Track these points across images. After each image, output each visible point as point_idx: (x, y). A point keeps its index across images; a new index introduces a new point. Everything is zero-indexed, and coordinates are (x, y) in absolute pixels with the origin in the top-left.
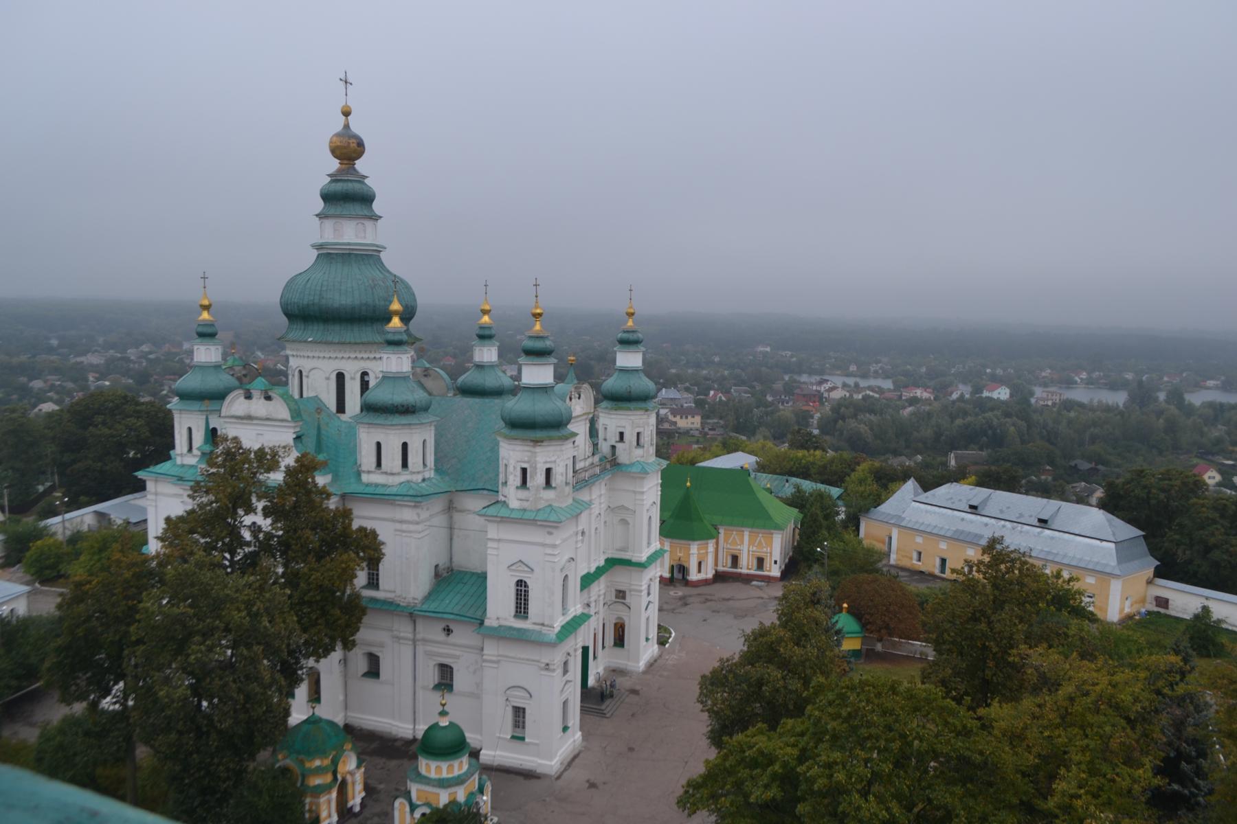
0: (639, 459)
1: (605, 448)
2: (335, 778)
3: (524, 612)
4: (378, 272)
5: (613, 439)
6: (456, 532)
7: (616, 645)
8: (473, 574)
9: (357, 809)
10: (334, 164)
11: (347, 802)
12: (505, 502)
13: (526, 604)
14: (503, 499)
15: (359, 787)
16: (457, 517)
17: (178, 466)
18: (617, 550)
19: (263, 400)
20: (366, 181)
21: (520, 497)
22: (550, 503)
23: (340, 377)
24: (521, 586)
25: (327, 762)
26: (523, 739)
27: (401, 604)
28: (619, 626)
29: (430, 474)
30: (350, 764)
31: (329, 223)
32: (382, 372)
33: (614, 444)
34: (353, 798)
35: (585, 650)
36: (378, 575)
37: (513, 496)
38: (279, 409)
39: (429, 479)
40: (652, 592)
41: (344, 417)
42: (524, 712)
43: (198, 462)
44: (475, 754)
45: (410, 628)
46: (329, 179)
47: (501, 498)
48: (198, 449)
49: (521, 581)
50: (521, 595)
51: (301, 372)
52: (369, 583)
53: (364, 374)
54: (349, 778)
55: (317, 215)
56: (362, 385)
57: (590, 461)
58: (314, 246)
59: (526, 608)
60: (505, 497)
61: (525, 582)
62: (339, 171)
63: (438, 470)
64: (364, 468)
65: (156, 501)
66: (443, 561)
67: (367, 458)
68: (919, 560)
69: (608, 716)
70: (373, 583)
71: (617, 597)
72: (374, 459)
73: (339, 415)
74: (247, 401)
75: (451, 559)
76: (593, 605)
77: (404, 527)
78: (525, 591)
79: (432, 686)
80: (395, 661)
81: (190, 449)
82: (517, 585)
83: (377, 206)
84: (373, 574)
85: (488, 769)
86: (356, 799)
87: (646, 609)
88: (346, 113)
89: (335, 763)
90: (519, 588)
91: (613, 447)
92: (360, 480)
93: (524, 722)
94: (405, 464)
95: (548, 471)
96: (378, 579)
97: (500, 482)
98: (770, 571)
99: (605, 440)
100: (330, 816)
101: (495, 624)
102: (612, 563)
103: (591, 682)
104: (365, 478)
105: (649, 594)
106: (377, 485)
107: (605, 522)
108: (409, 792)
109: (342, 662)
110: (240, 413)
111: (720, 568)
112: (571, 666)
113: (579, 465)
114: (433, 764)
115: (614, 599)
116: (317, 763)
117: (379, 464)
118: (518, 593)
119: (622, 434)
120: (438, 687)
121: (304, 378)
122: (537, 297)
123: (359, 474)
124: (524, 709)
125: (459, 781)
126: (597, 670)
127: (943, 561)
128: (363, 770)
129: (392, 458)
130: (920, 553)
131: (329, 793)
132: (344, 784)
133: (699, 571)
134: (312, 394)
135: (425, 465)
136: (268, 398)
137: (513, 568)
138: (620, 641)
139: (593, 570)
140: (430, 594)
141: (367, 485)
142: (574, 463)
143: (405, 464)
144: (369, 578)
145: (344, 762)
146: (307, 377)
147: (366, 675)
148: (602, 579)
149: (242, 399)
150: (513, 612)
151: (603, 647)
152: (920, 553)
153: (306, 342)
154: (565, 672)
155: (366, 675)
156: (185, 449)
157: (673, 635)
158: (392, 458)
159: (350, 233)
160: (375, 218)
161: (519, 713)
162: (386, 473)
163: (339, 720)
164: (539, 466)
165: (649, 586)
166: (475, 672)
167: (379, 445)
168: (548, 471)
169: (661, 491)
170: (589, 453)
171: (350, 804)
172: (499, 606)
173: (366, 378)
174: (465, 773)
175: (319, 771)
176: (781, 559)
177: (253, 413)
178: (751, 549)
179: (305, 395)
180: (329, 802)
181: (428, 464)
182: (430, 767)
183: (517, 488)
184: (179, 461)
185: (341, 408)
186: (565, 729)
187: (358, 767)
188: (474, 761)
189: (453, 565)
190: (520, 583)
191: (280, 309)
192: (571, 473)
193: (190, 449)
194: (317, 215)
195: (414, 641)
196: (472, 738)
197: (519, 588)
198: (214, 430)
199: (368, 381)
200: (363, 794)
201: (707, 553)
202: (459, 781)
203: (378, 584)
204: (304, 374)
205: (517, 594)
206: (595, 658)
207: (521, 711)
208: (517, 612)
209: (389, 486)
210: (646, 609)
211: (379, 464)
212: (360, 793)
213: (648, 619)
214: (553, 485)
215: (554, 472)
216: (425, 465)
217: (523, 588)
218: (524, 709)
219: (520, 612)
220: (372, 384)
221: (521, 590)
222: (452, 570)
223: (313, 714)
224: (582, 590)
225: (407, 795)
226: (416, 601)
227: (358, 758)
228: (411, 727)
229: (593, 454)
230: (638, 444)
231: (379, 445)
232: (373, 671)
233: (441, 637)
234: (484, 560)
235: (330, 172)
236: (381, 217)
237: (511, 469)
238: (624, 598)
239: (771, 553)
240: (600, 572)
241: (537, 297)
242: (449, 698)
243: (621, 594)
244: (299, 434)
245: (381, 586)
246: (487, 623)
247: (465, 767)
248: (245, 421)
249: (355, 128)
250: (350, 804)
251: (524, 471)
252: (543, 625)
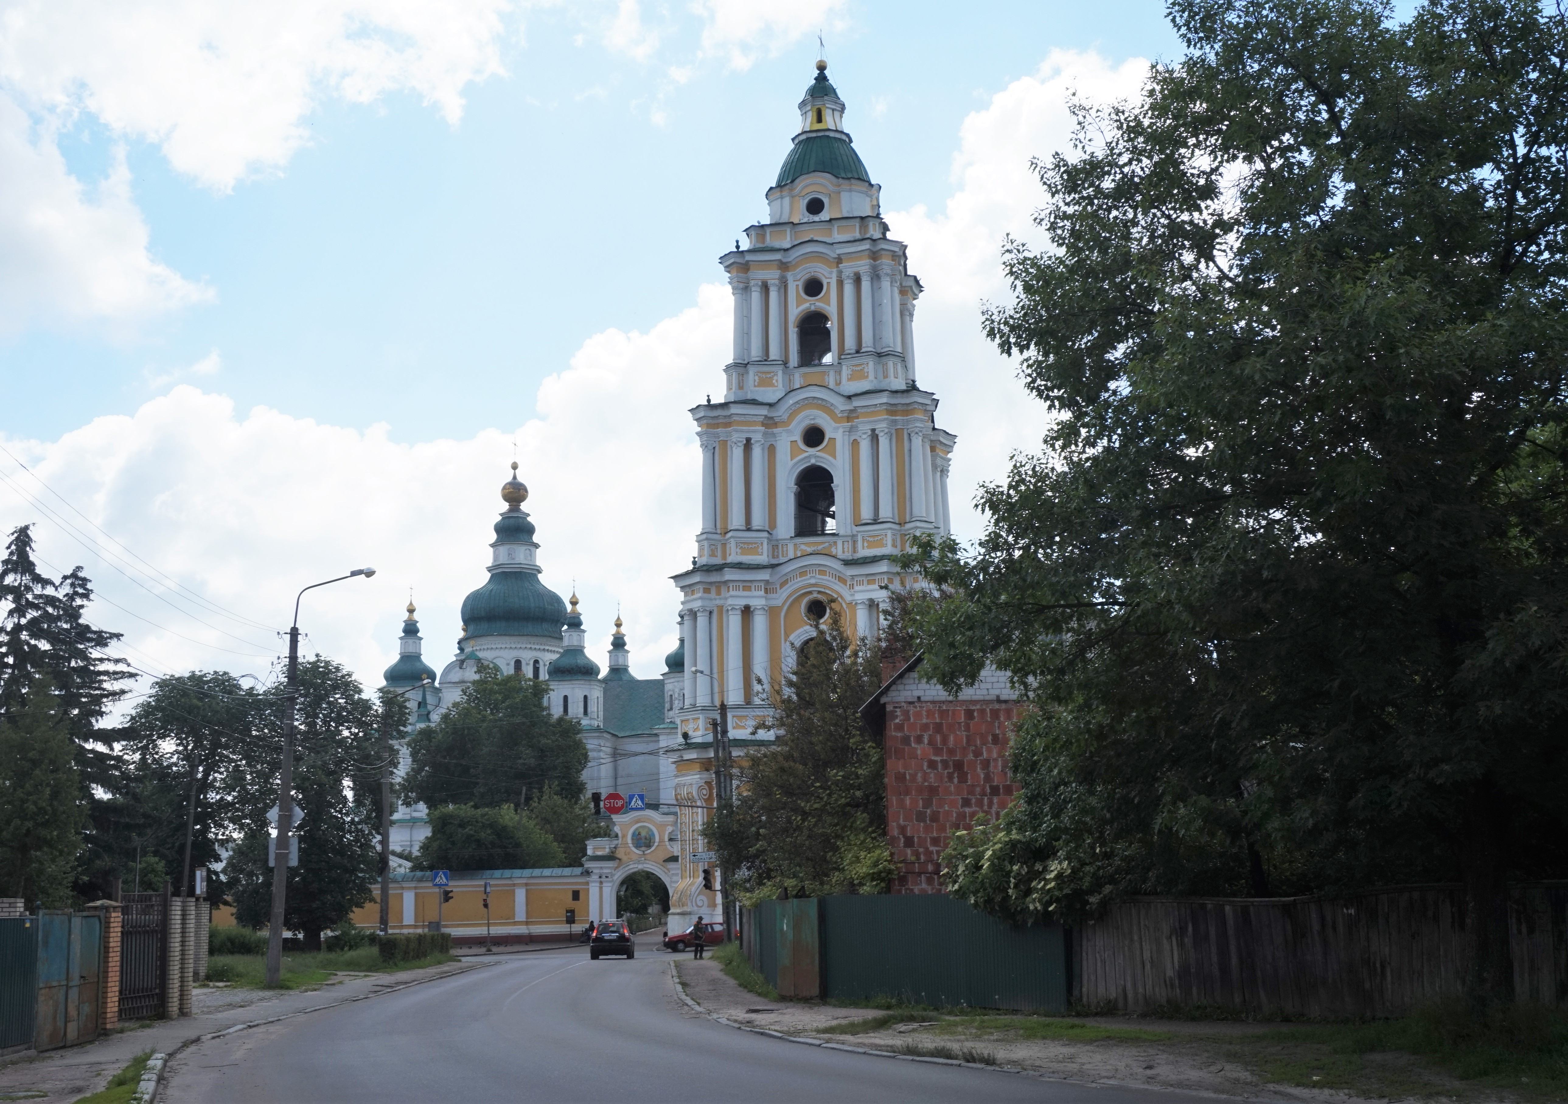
10: (505, 506)
20: (529, 519)
31: (503, 549)
46: (500, 518)
53: (536, 662)
83: (536, 538)
88: (515, 467)
159: (520, 555)
249: (520, 479)
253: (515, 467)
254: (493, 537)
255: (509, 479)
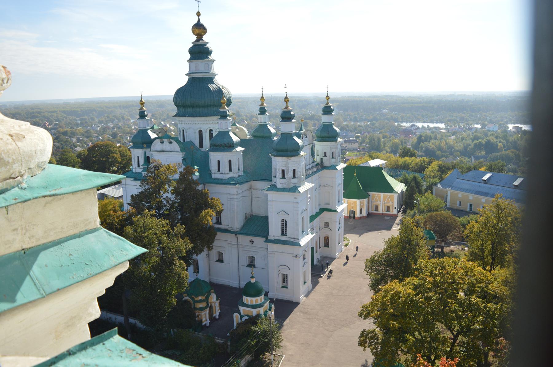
0: (333, 164)
1: (317, 159)
2: (208, 304)
3: (285, 233)
4: (215, 85)
5: (321, 155)
6: (254, 199)
7: (325, 246)
8: (262, 217)
9: (217, 317)
11: (213, 314)
12: (275, 185)
13: (286, 230)
14: (274, 184)
15: (218, 308)
16: (254, 191)
17: (134, 173)
18: (325, 204)
19: (168, 143)
20: (208, 45)
21: (281, 183)
22: (295, 185)
23: (200, 132)
24: (284, 222)
25: (204, 298)
26: (287, 288)
27: (232, 231)
28: (327, 238)
29: (241, 173)
30: (213, 298)
32: (219, 129)
33: (322, 157)
34: (216, 313)
35: (312, 248)
36: (220, 218)
37: (279, 182)
38: (175, 146)
39: (241, 176)
40: (341, 223)
41: (202, 150)
42: (287, 276)
43: (142, 171)
44: (266, 294)
45: (236, 241)
46: (192, 45)
47: (273, 183)
48: (142, 165)
49: (284, 219)
50: (284, 226)
51: (183, 131)
52: (217, 221)
53: (211, 130)
54: (213, 304)
55: (187, 61)
56: (210, 135)
57: (311, 166)
58: (187, 75)
59: (286, 232)
60: (275, 183)
61: (285, 220)
62: (196, 41)
63: (244, 172)
64: (213, 172)
65: (126, 188)
66: (248, 212)
67: (214, 167)
68: (460, 205)
69: (323, 277)
70: (219, 222)
71: (325, 225)
72: (217, 168)
73: (200, 149)
74: (161, 144)
75: (252, 210)
76: (315, 229)
77: (231, 197)
78: (285, 224)
79: (246, 265)
80: (230, 255)
81: (139, 166)
82: (282, 222)
83: (212, 57)
84: (219, 218)
85: (272, 301)
86: (217, 314)
87: (338, 230)
88: (198, 14)
89: (207, 298)
90: (283, 223)
91: (322, 159)
92: (211, 177)
93: (287, 281)
94: (230, 170)
95: (294, 171)
96: (221, 220)
97: (273, 176)
98: (393, 212)
99: (318, 155)
100: (206, 320)
101: (273, 238)
102: (322, 210)
103: (315, 263)
104: (214, 176)
105: (339, 224)
106: (218, 179)
107: (319, 193)
108: (240, 311)
109: (207, 255)
110: (160, 150)
111: (370, 211)
112: (306, 257)
113: (308, 167)
114: (250, 299)
115: (324, 226)
116: (200, 298)
117: (219, 170)
118: (282, 225)
119: (325, 153)
120: (249, 266)
121: (185, 134)
122: (286, 92)
123: (210, 174)
124: (287, 275)
125: (261, 306)
126: (317, 256)
127: (471, 205)
128: (219, 301)
129: (225, 167)
130: (460, 202)
131: (206, 311)
132: (211, 307)
133: (361, 213)
134: (189, 140)
135: (239, 170)
136: (171, 143)
137: (280, 213)
138: (327, 245)
139: (314, 214)
140: (244, 226)
141: (215, 179)
142: (305, 166)
143: (230, 170)
144: (217, 220)
145: (211, 298)
146: (186, 132)
147: (217, 261)
148: (318, 218)
149: (159, 143)
150: (280, 233)
151: (320, 247)
152: (460, 202)
153: (185, 116)
154: (304, 259)
155: (217, 261)
156: (137, 166)
157: (350, 242)
158: (225, 167)
160: (213, 61)
161: (285, 277)
162: (222, 174)
163: (207, 280)
164: (290, 168)
165: (339, 220)
166: (264, 259)
167: (219, 161)
168: (294, 171)
169: (344, 178)
170: (311, 162)
171: (214, 316)
172: (274, 230)
173: (212, 132)
174: (264, 302)
175: (201, 301)
176: (397, 207)
177: (164, 150)
178: (384, 203)
179: (185, 141)
180: (206, 314)
181: (240, 169)
182: (247, 300)
183: (280, 178)
184: (134, 171)
185: (201, 145)
186: (305, 283)
187: (217, 300)
188: (266, 297)
189: (253, 213)
190: (283, 220)
191: (173, 103)
192: (304, 172)
193: (139, 166)
194: (187, 61)
195: (238, 247)
196: (265, 288)
197: (283, 223)
198: (148, 157)
199: (212, 133)
200: (220, 311)
201: (364, 205)
202: (261, 306)
203: (221, 222)
204: (185, 131)
205: (282, 225)
206: (316, 252)
207: (286, 276)
208: (282, 233)
209: (224, 180)
210: (338, 230)
211: (219, 170)
212: (218, 310)
213: (339, 235)
214: (296, 177)
215: (296, 171)
216: (239, 170)
217: (284, 223)
218: (287, 275)
219: (284, 233)
220: (214, 135)
221: (284, 224)
222: (253, 215)
223: (197, 278)
224: (310, 223)
225: (239, 312)
226: (238, 229)
227: (217, 296)
228: (238, 283)
229: (313, 162)
230: (333, 158)
231: (219, 161)
232: (221, 260)
233: (250, 244)
234: (267, 210)
235: (192, 42)
236: (215, 60)
237: (278, 170)
238: (328, 226)
239: (393, 203)
240: (318, 214)
241: (286, 92)
242: (254, 269)
243: (327, 225)
244: (185, 157)
245: (222, 224)
246: (269, 238)
247: (263, 300)
248: (161, 153)
249: (202, 22)
250: (214, 316)
251: (283, 171)
252: (294, 238)
253: (198, 14)
254: (189, 56)
255: (196, 22)
